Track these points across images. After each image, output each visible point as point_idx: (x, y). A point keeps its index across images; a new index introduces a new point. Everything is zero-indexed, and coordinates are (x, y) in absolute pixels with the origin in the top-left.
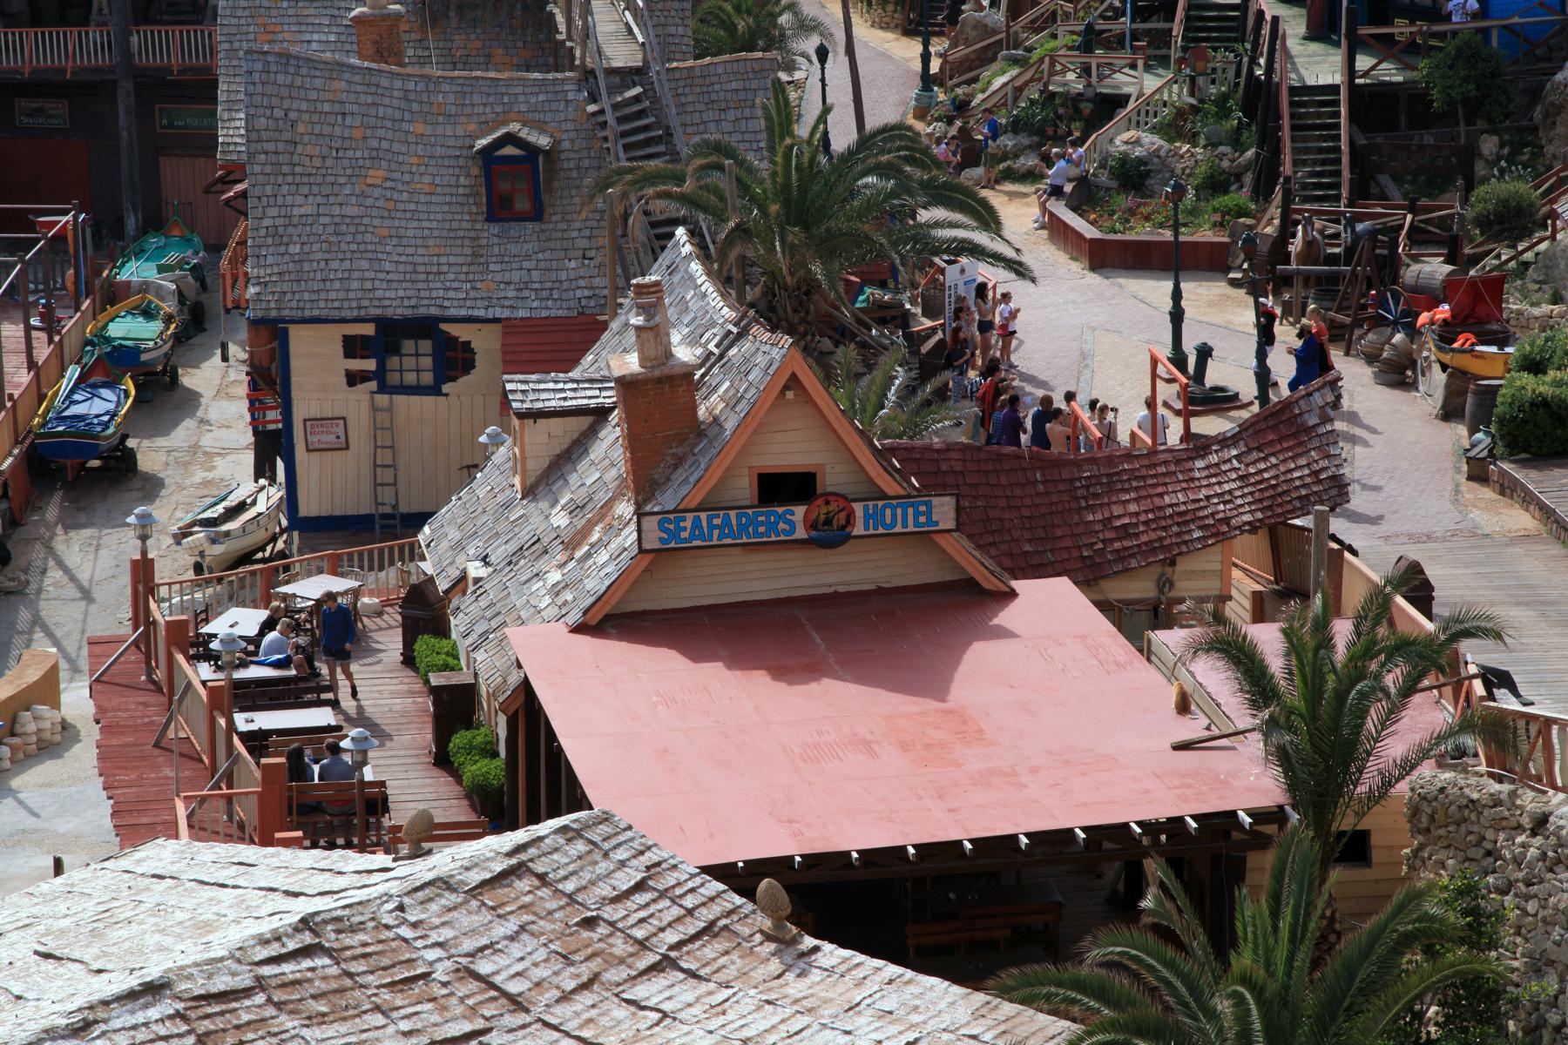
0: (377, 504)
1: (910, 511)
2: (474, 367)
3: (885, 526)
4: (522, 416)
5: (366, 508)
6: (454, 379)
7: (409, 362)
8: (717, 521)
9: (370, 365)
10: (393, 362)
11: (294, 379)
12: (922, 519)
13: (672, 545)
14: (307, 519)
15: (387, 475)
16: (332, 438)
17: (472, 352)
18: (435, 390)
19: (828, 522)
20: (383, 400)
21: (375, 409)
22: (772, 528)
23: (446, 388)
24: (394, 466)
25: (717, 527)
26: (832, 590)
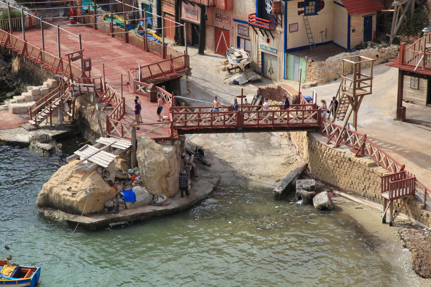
0: (310, 43)
2: (324, 7)
4: (81, 49)
5: (308, 44)
6: (319, 10)
7: (310, 7)
9: (303, 9)
10: (307, 8)
11: (288, 15)
14: (289, 49)
15: (310, 36)
16: (295, 28)
17: (324, 3)
18: (316, 14)
20: (306, 17)
21: (304, 20)
23: (318, 13)
24: (311, 33)
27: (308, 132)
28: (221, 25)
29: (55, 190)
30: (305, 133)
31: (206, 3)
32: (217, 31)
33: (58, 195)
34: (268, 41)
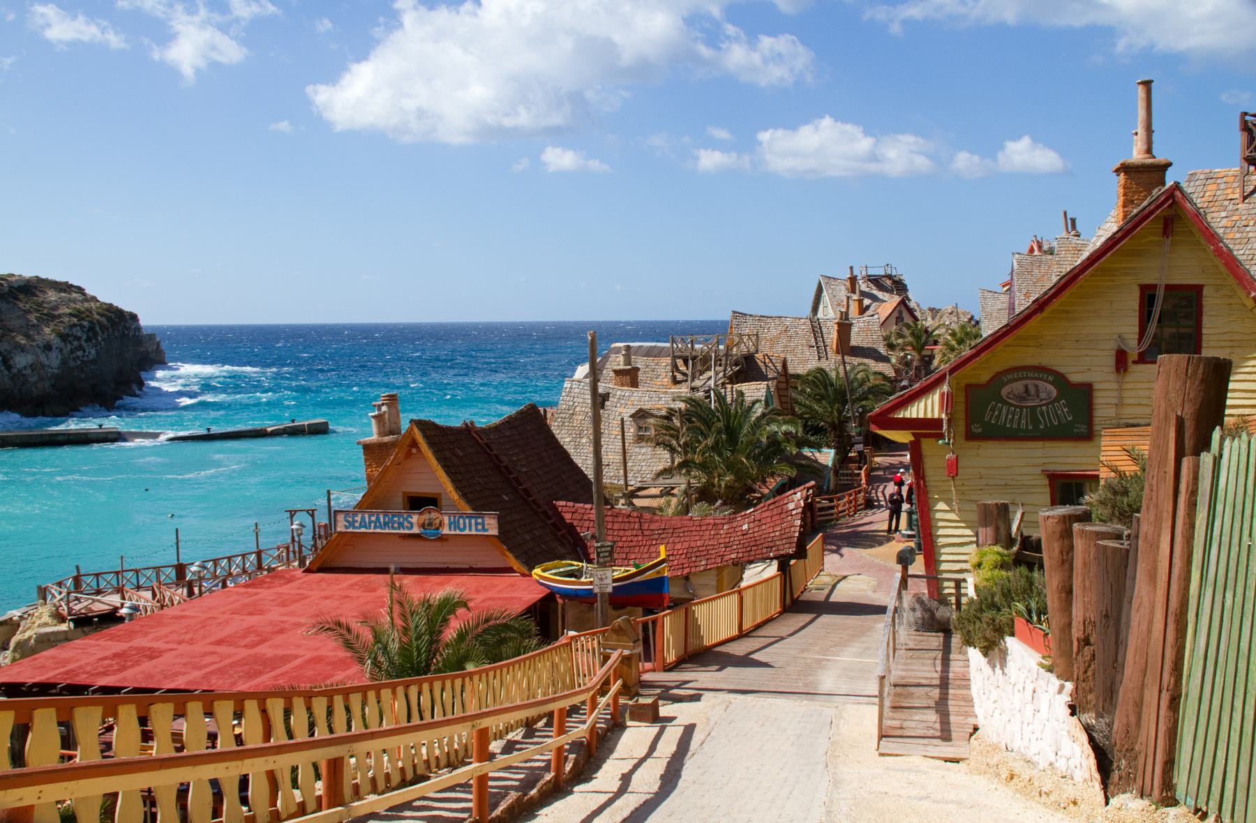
1: (473, 521)
3: (461, 530)
8: (373, 518)
12: (480, 527)
13: (351, 530)
19: (430, 524)
22: (401, 525)
25: (373, 522)
26: (445, 566)
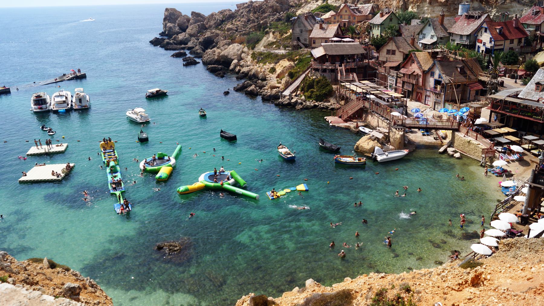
27: (453, 132)
28: (419, 91)
29: (361, 144)
30: (451, 131)
31: (414, 83)
32: (418, 93)
33: (361, 146)
34: (438, 97)
